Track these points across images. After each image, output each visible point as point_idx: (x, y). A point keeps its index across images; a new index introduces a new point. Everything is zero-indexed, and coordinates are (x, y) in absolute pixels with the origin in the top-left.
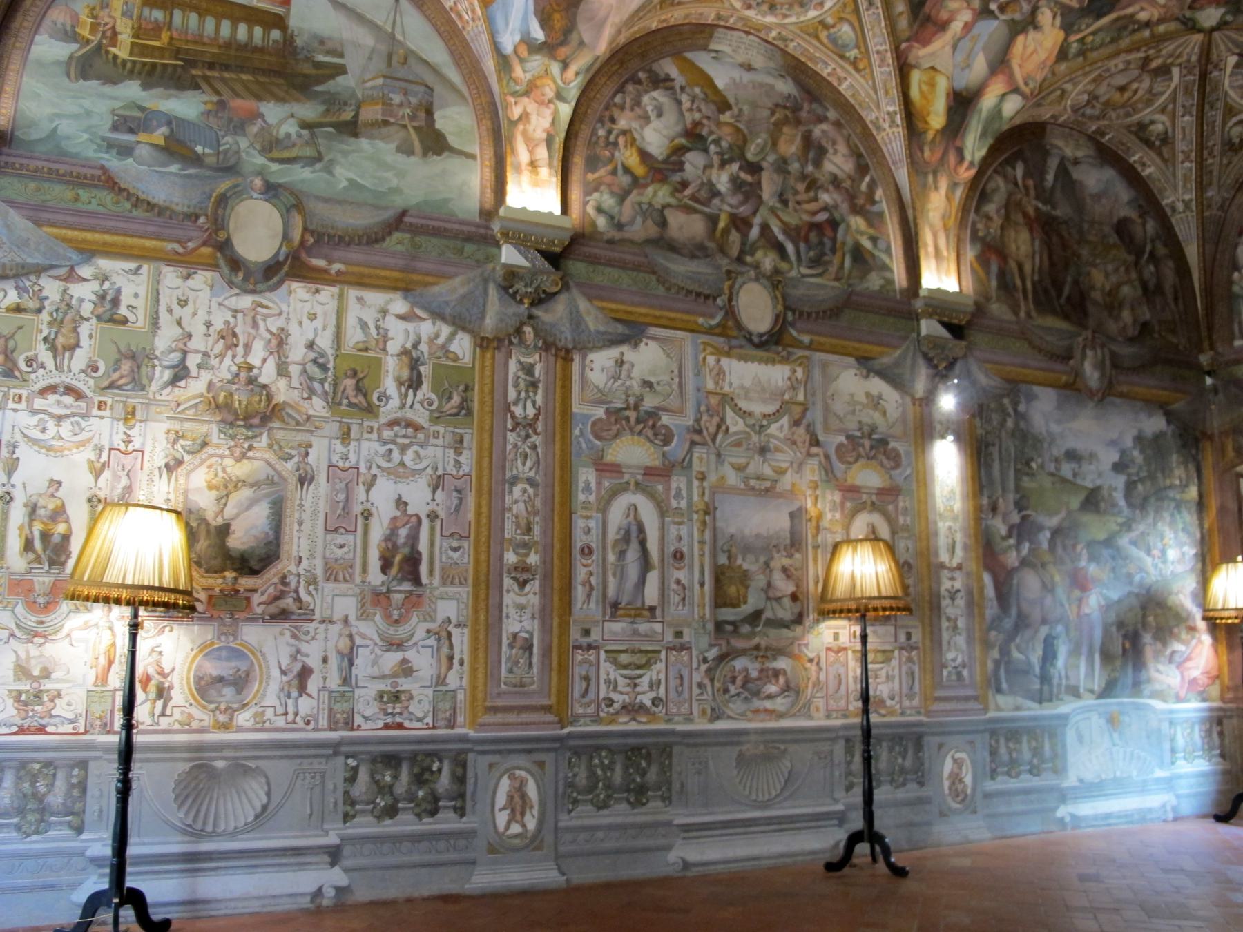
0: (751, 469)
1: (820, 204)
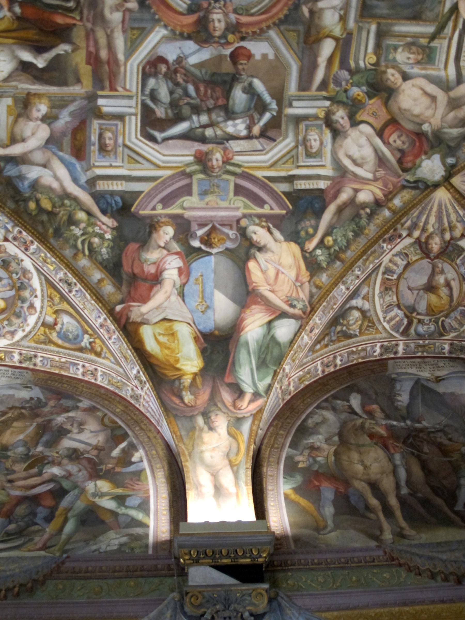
1: (46, 476)
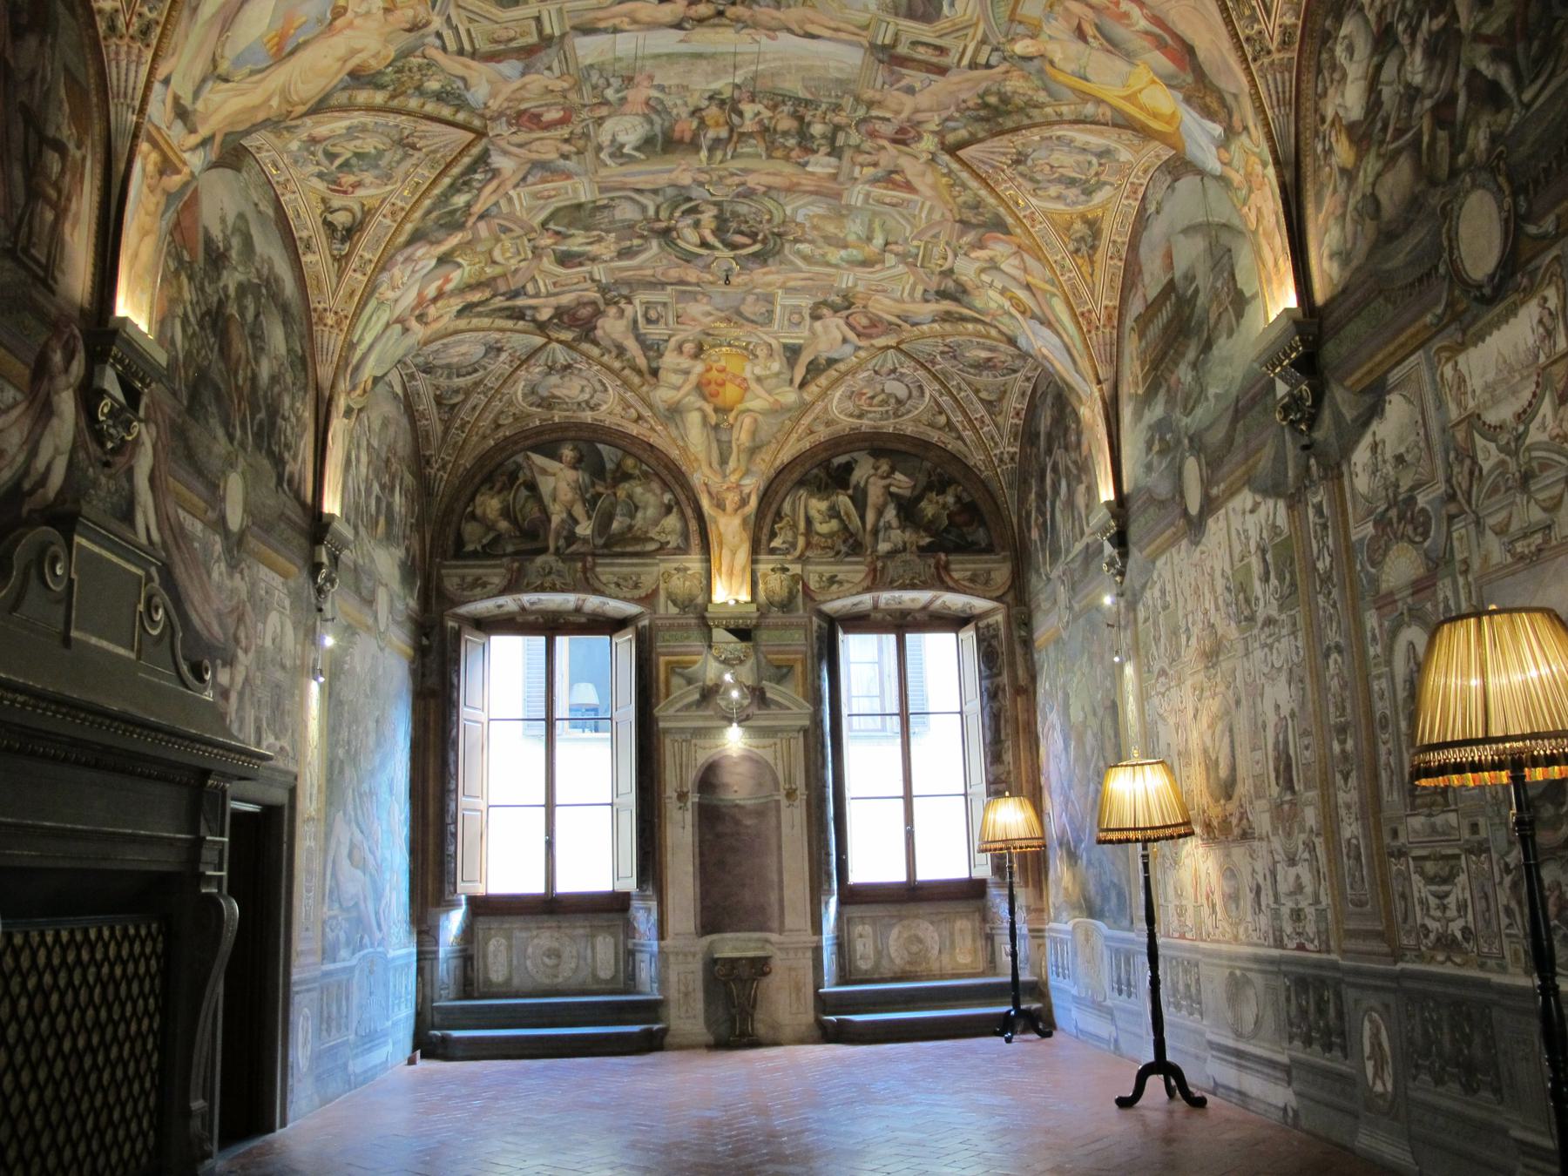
0: (1514, 527)
